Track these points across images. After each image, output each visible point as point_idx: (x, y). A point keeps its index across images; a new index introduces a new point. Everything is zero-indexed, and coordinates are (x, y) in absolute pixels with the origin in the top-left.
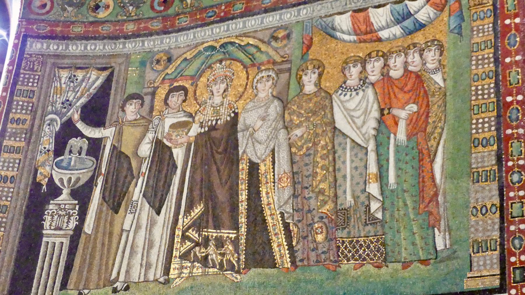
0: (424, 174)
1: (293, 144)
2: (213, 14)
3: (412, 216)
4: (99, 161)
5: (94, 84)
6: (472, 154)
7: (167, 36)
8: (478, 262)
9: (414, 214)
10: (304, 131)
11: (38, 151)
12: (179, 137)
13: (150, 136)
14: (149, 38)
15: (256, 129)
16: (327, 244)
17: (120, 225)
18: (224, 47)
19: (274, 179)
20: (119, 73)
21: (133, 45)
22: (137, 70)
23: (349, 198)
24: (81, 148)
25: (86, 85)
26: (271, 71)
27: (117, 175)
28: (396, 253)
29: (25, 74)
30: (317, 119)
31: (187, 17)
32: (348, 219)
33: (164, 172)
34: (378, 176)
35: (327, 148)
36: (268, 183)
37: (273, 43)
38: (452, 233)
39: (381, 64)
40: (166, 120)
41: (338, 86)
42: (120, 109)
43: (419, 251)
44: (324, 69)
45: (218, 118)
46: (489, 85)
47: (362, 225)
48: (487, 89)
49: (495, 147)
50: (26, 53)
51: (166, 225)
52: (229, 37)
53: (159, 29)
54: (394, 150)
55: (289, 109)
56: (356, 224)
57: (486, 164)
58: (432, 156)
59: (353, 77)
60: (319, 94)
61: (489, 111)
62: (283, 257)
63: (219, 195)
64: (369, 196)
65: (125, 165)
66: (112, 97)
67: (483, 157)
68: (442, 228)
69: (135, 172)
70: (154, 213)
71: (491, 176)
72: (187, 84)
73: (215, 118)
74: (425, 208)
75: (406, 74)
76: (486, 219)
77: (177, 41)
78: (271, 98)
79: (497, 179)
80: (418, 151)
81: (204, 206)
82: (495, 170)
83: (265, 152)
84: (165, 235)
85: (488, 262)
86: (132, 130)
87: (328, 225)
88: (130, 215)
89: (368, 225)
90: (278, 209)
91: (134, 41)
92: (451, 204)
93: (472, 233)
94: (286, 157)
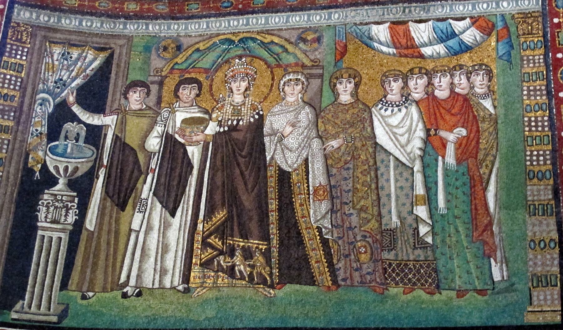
0: (477, 202)
1: (329, 155)
2: (230, 4)
3: (465, 244)
4: (100, 151)
5: (90, 66)
6: (527, 186)
7: (175, 22)
8: (538, 296)
9: (468, 242)
10: (341, 143)
11: (29, 133)
12: (193, 134)
13: (159, 129)
14: (154, 21)
15: (285, 135)
16: (373, 265)
17: (127, 225)
18: (244, 42)
19: (308, 190)
20: (119, 56)
21: (136, 27)
22: (141, 55)
23: (395, 219)
24: (78, 134)
25: (82, 64)
26: (300, 74)
27: (121, 169)
28: (449, 280)
29: (12, 45)
30: (355, 131)
31: (198, 4)
32: (394, 241)
33: (178, 171)
34: (427, 199)
35: (368, 164)
36: (302, 194)
37: (301, 45)
38: (510, 265)
39: (425, 82)
40: (177, 113)
41: (377, 99)
42: (122, 96)
43: (474, 280)
44: (361, 80)
45: (240, 118)
46: (543, 117)
47: (410, 247)
48: (541, 121)
49: (551, 182)
50: (13, 21)
51: (182, 228)
52: (250, 32)
53: (165, 13)
54: (443, 174)
55: (322, 118)
56: (404, 247)
57: (542, 198)
58: (484, 184)
59: (394, 92)
60: (356, 106)
61: (544, 144)
62: (323, 274)
63: (244, 202)
64: (417, 219)
65: (131, 159)
66: (112, 81)
67: (539, 191)
68: (499, 259)
69: (143, 168)
70: (168, 215)
71: (549, 211)
72: (201, 78)
73: (237, 118)
74: (479, 236)
75: (452, 96)
76: (545, 254)
77: (186, 28)
78: (302, 104)
79: (554, 214)
80: (469, 177)
81: (228, 212)
82: (552, 205)
83: (297, 161)
84: (181, 240)
85: (549, 297)
86: (136, 120)
87: (372, 244)
88: (139, 213)
89: (417, 248)
90: (314, 223)
91: (136, 22)
92: (506, 234)
93: (530, 266)
94: (321, 168)
